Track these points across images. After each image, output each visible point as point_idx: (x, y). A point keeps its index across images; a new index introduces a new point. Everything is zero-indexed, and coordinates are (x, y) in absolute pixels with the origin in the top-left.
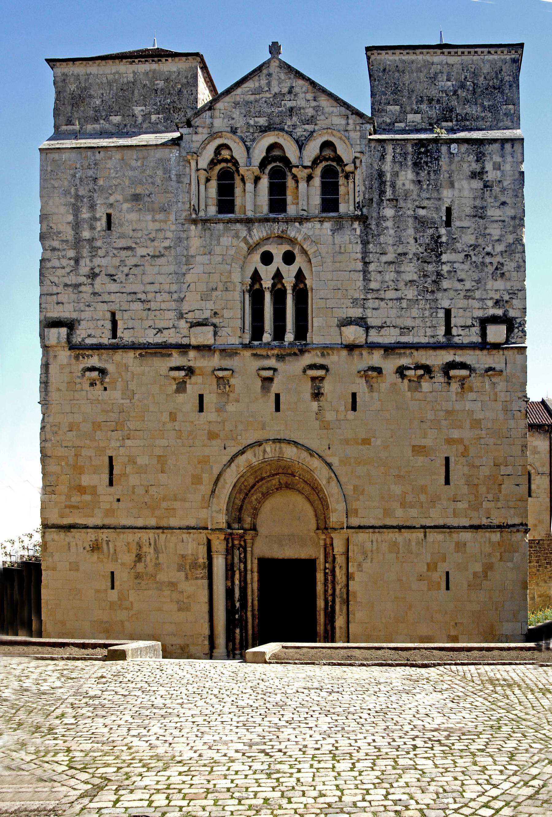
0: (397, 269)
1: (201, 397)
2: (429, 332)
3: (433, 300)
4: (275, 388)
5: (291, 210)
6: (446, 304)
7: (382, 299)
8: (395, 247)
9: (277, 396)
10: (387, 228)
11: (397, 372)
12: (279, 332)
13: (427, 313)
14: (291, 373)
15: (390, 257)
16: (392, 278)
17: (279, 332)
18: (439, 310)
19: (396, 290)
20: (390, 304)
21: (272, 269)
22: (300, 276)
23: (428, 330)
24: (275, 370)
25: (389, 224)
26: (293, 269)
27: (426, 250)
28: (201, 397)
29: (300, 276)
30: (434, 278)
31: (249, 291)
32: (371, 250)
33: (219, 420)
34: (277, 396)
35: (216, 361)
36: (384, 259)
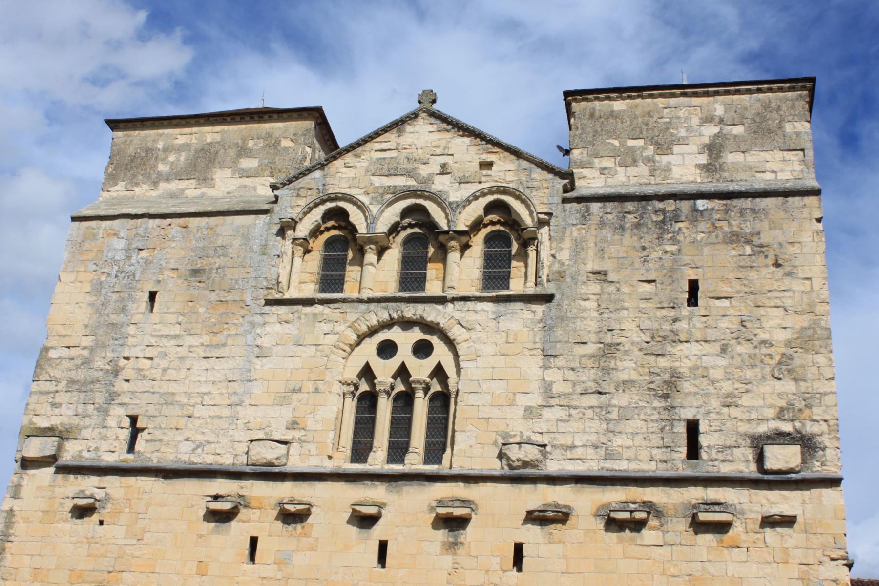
0: (602, 364)
1: (254, 541)
2: (658, 454)
3: (666, 409)
4: (378, 532)
5: (433, 288)
6: (689, 414)
7: (575, 408)
8: (601, 335)
9: (383, 546)
10: (585, 310)
11: (596, 515)
12: (398, 449)
13: (654, 427)
14: (407, 511)
15: (591, 349)
16: (593, 377)
17: (398, 449)
18: (676, 423)
19: (600, 393)
20: (589, 413)
21: (394, 364)
22: (439, 372)
23: (655, 451)
24: (381, 506)
25: (592, 304)
26: (429, 364)
27: (653, 338)
28: (254, 541)
29: (439, 372)
30: (666, 377)
31: (353, 394)
32: (559, 338)
33: (279, 575)
34: (383, 546)
35: (286, 490)
36: (580, 350)
